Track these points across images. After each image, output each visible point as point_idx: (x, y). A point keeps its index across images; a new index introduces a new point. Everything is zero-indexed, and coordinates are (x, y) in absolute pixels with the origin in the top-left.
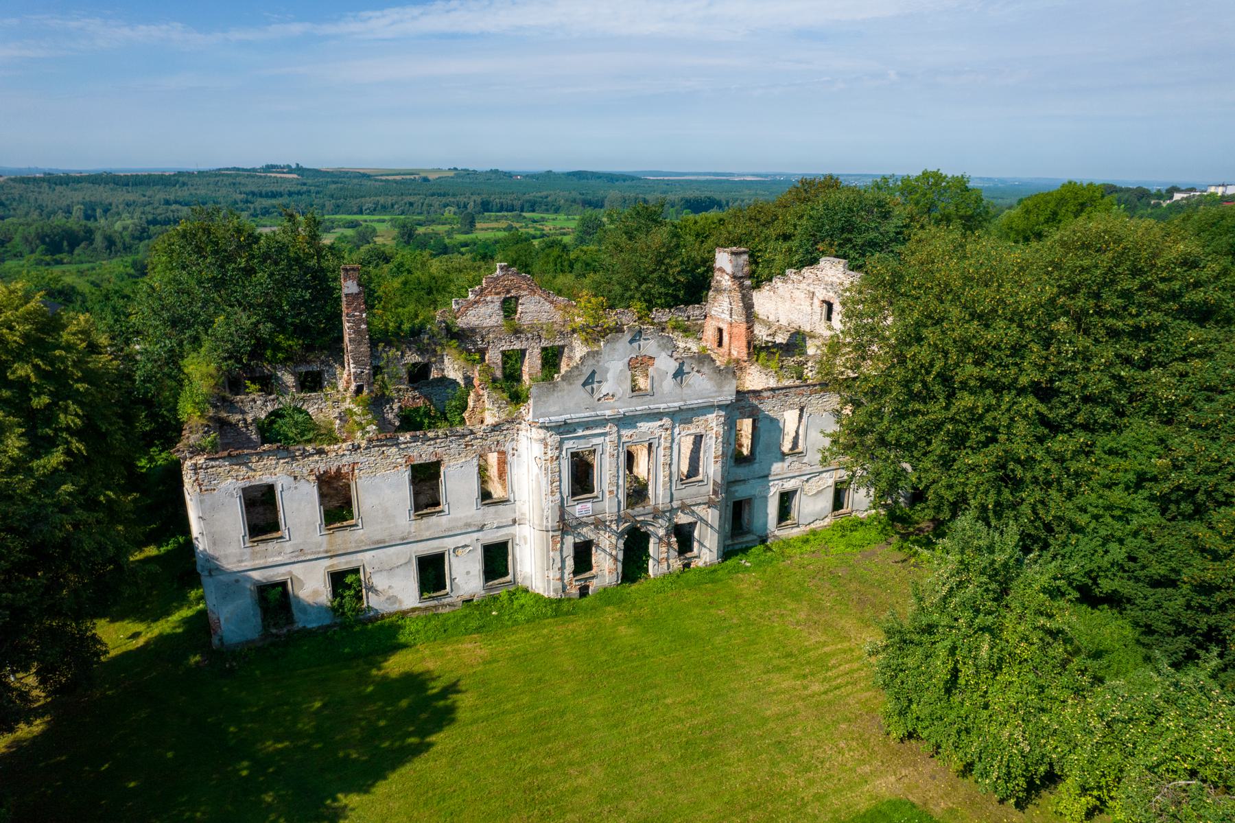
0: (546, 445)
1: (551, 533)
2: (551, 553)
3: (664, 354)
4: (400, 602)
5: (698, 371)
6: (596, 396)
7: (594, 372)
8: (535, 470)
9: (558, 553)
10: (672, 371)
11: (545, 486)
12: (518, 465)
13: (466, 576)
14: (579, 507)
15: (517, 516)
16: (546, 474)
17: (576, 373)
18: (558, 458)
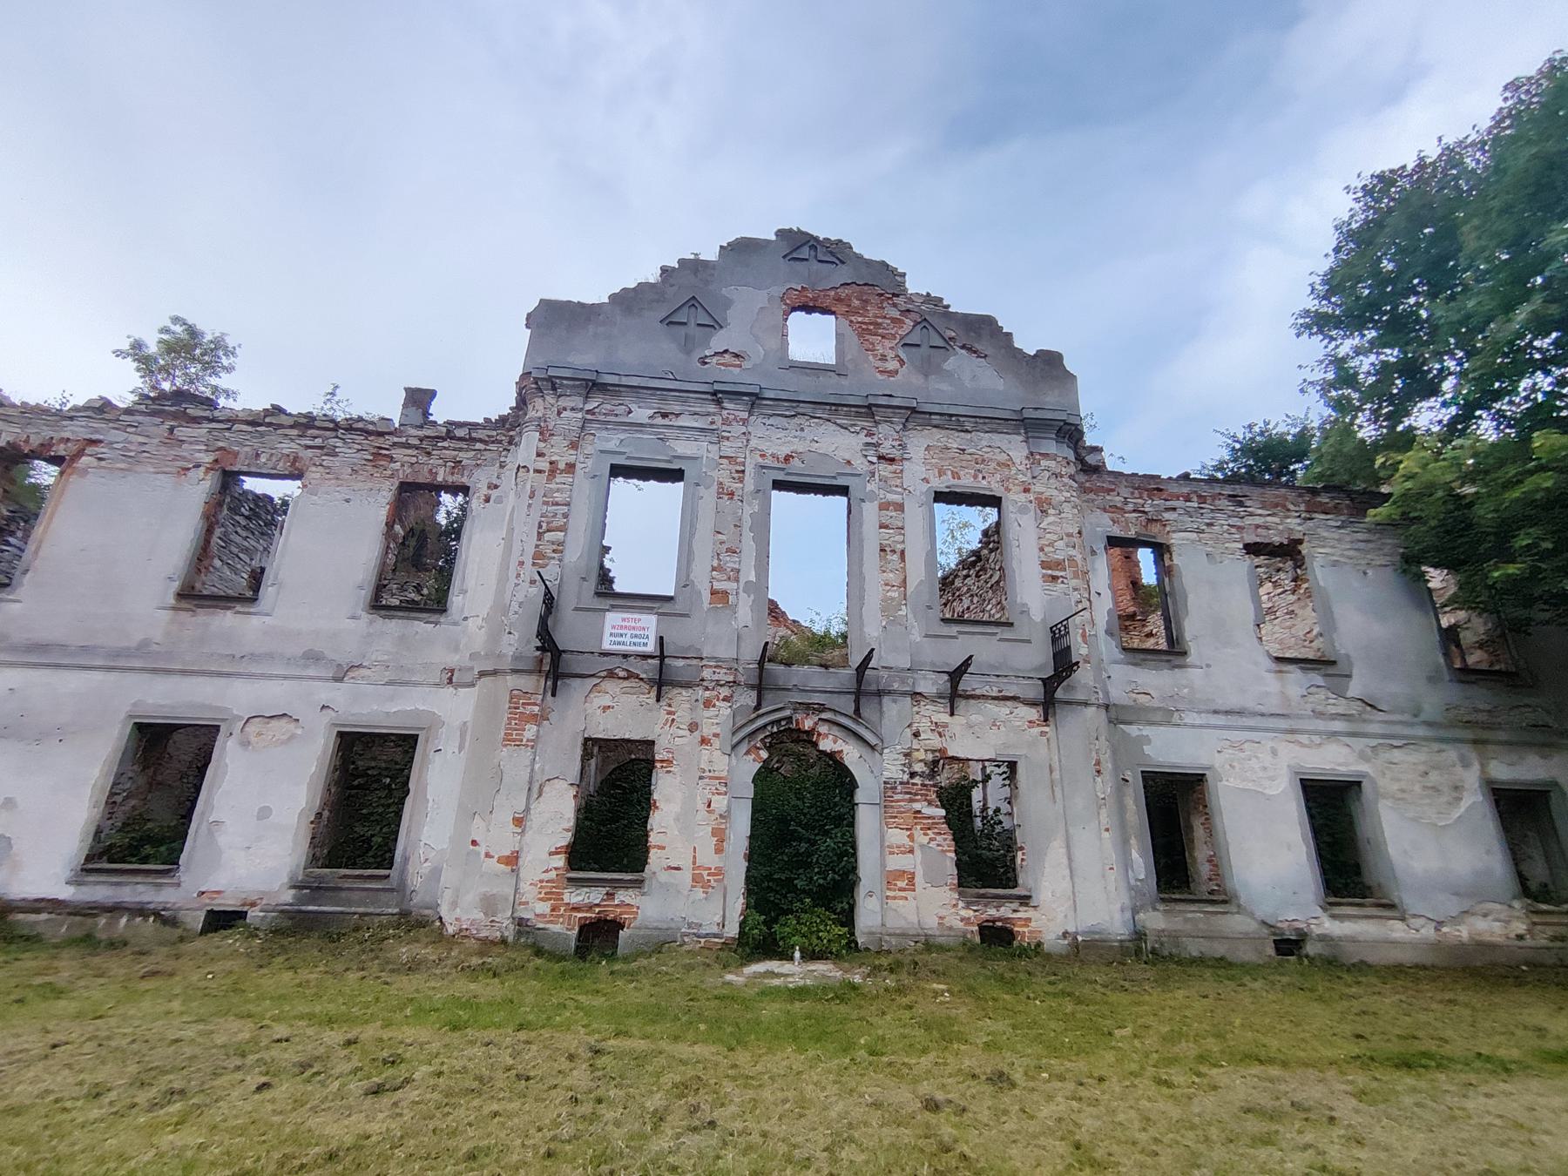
7: (693, 303)
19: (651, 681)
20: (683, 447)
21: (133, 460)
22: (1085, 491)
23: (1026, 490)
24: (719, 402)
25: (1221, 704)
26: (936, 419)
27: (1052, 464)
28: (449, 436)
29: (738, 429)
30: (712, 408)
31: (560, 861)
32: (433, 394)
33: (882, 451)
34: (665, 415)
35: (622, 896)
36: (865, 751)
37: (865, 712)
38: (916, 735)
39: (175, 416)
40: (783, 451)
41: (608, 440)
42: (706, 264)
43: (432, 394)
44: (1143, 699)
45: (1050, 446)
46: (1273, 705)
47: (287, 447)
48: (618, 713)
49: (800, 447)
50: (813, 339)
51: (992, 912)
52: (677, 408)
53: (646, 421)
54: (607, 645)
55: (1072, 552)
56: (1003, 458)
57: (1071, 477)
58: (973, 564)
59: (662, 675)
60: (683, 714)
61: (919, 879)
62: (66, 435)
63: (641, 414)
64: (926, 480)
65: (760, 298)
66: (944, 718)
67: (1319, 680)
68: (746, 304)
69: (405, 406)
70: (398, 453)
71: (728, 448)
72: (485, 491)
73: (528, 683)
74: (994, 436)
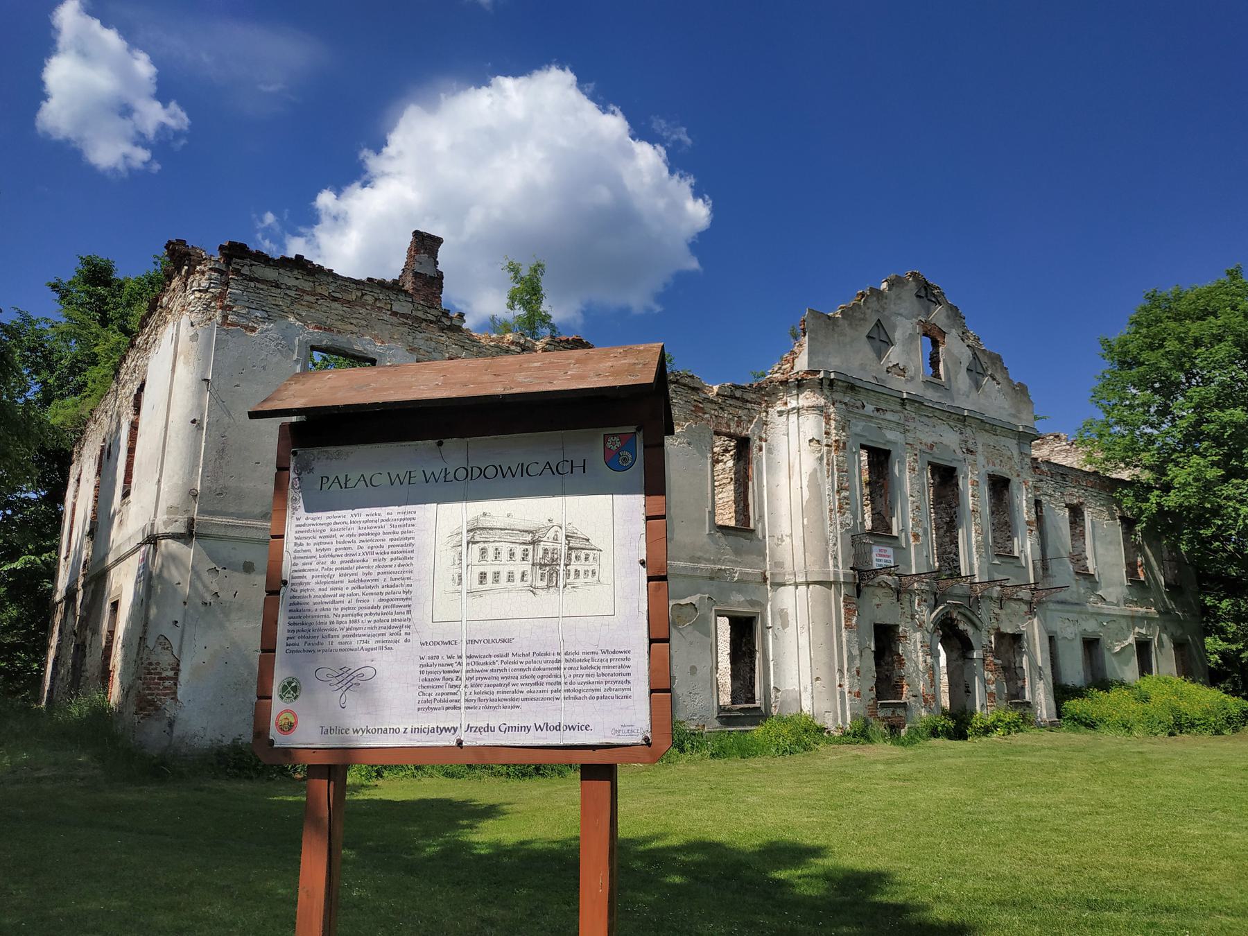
0: (828, 418)
2: (844, 634)
14: (876, 550)
30: (899, 408)
34: (878, 410)
40: (929, 441)
43: (438, 241)
48: (882, 608)
60: (907, 610)
66: (997, 611)
70: (707, 406)
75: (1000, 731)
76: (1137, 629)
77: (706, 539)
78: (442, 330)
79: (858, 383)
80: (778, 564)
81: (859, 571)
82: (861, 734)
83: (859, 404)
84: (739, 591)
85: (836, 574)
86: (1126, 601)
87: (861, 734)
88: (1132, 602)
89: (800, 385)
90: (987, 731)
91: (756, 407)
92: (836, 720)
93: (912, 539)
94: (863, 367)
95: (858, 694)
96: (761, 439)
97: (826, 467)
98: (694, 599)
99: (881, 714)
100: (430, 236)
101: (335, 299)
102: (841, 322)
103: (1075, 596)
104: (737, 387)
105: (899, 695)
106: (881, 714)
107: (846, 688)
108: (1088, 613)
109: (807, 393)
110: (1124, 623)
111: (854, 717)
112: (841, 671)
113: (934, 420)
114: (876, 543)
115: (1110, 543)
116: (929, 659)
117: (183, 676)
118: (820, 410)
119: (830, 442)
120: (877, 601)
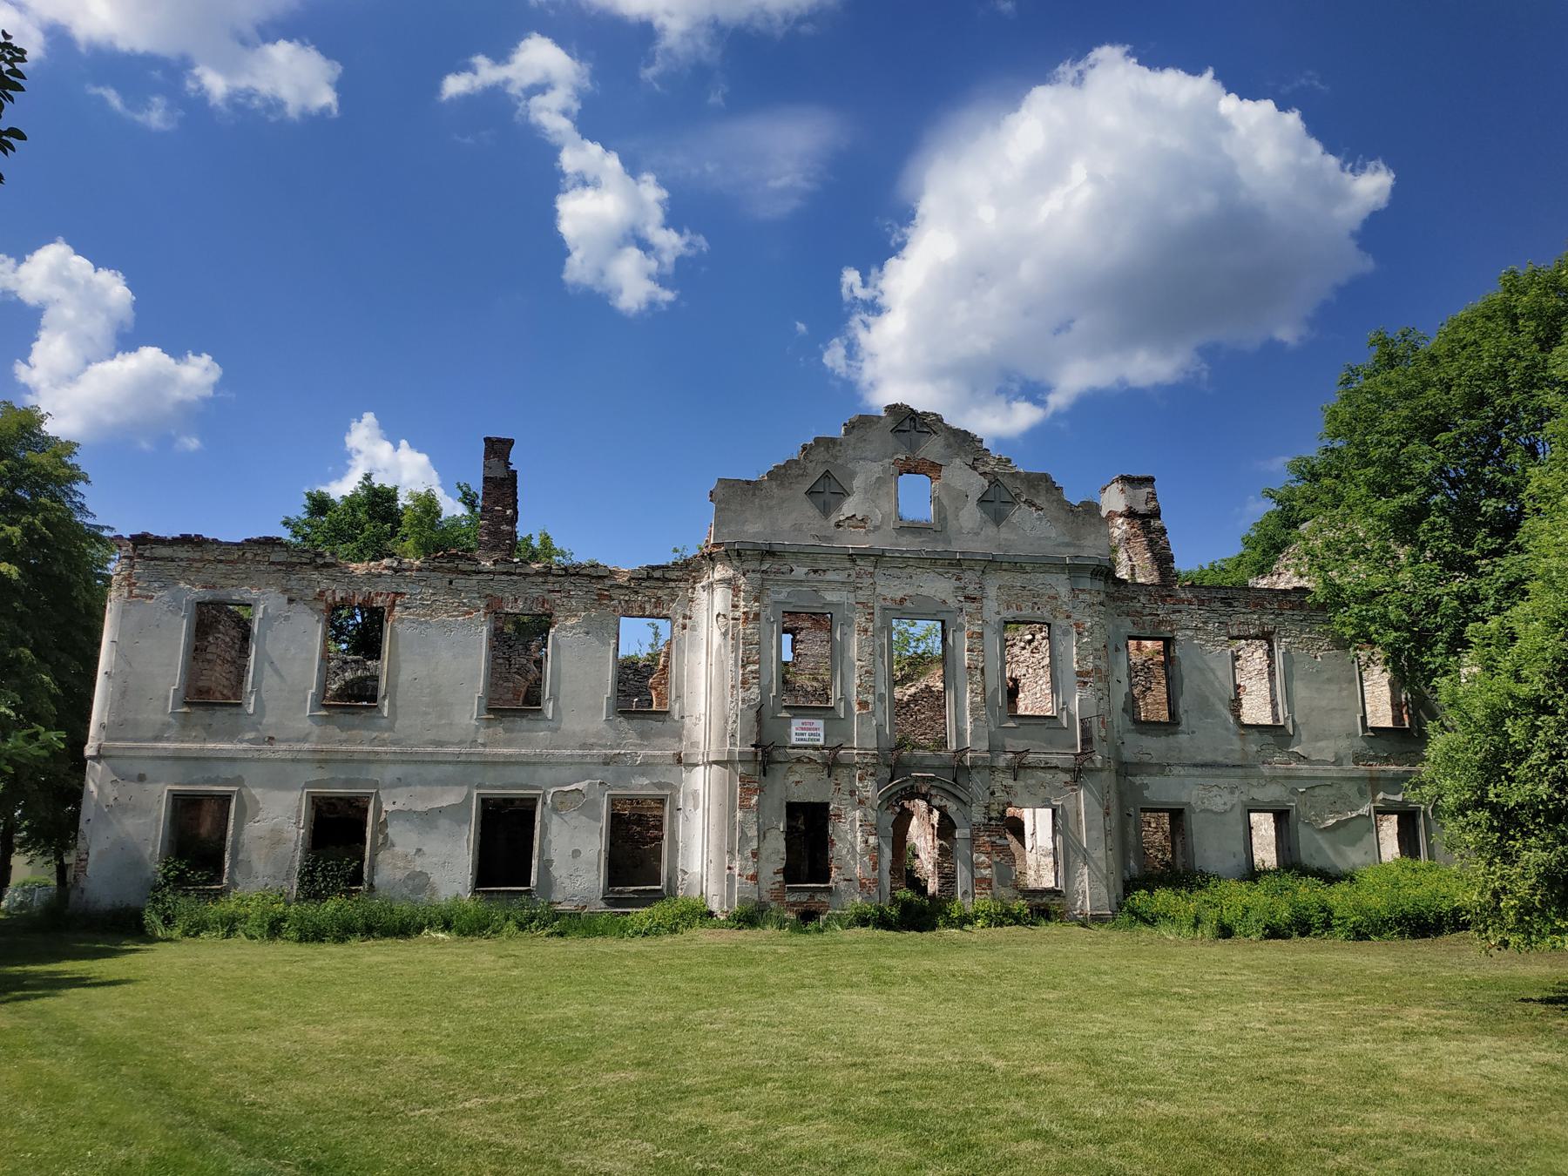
0: (736, 591)
1: (740, 769)
2: (739, 814)
3: (958, 461)
4: (434, 891)
5: (1031, 504)
6: (833, 519)
8: (717, 638)
9: (752, 817)
10: (975, 494)
11: (733, 673)
12: (691, 645)
13: (572, 854)
14: (796, 724)
15: (684, 747)
16: (735, 649)
17: (795, 471)
18: (757, 616)
19: (825, 764)
20: (831, 597)
21: (432, 609)
22: (1114, 599)
23: (1068, 617)
24: (854, 561)
25: (1199, 759)
26: (1005, 566)
27: (1087, 597)
28: (649, 578)
29: (867, 581)
30: (848, 565)
31: (780, 878)
32: (510, 442)
33: (967, 592)
34: (815, 572)
35: (818, 897)
36: (960, 805)
37: (960, 780)
38: (993, 793)
39: (449, 571)
40: (900, 595)
41: (779, 593)
42: (833, 441)
43: (509, 443)
44: (1146, 758)
45: (1086, 583)
46: (1235, 758)
47: (536, 592)
48: (805, 786)
49: (909, 591)
50: (916, 498)
51: (1038, 901)
52: (824, 566)
53: (803, 577)
54: (794, 741)
55: (1098, 662)
56: (1052, 593)
57: (1101, 604)
58: (1030, 642)
59: (832, 764)
60: (845, 786)
61: (994, 883)
62: (379, 589)
63: (800, 572)
64: (998, 613)
65: (876, 469)
66: (1011, 782)
67: (1270, 739)
68: (864, 475)
69: (487, 457)
70: (615, 593)
71: (862, 596)
72: (681, 620)
73: (750, 768)
74: (1047, 576)
75: (980, 922)
76: (1381, 796)
77: (603, 725)
78: (316, 568)
79: (776, 548)
80: (694, 744)
81: (764, 748)
82: (749, 918)
83: (785, 569)
84: (643, 775)
85: (730, 752)
86: (1358, 759)
87: (749, 918)
88: (1376, 758)
89: (711, 558)
90: (965, 921)
91: (682, 584)
92: (722, 904)
93: (856, 707)
94: (797, 528)
95: (754, 877)
96: (685, 617)
97: (731, 642)
98: (581, 785)
99: (792, 898)
100: (499, 440)
101: (221, 561)
102: (766, 484)
103: (1238, 756)
104: (654, 568)
105: (827, 879)
106: (792, 898)
107: (737, 871)
108: (1262, 776)
109: (719, 567)
110: (1351, 790)
111: (742, 901)
112: (731, 852)
113: (908, 570)
114: (795, 716)
115: (1329, 680)
116: (872, 840)
117: (91, 859)
118: (728, 582)
119: (737, 614)
120: (797, 778)
